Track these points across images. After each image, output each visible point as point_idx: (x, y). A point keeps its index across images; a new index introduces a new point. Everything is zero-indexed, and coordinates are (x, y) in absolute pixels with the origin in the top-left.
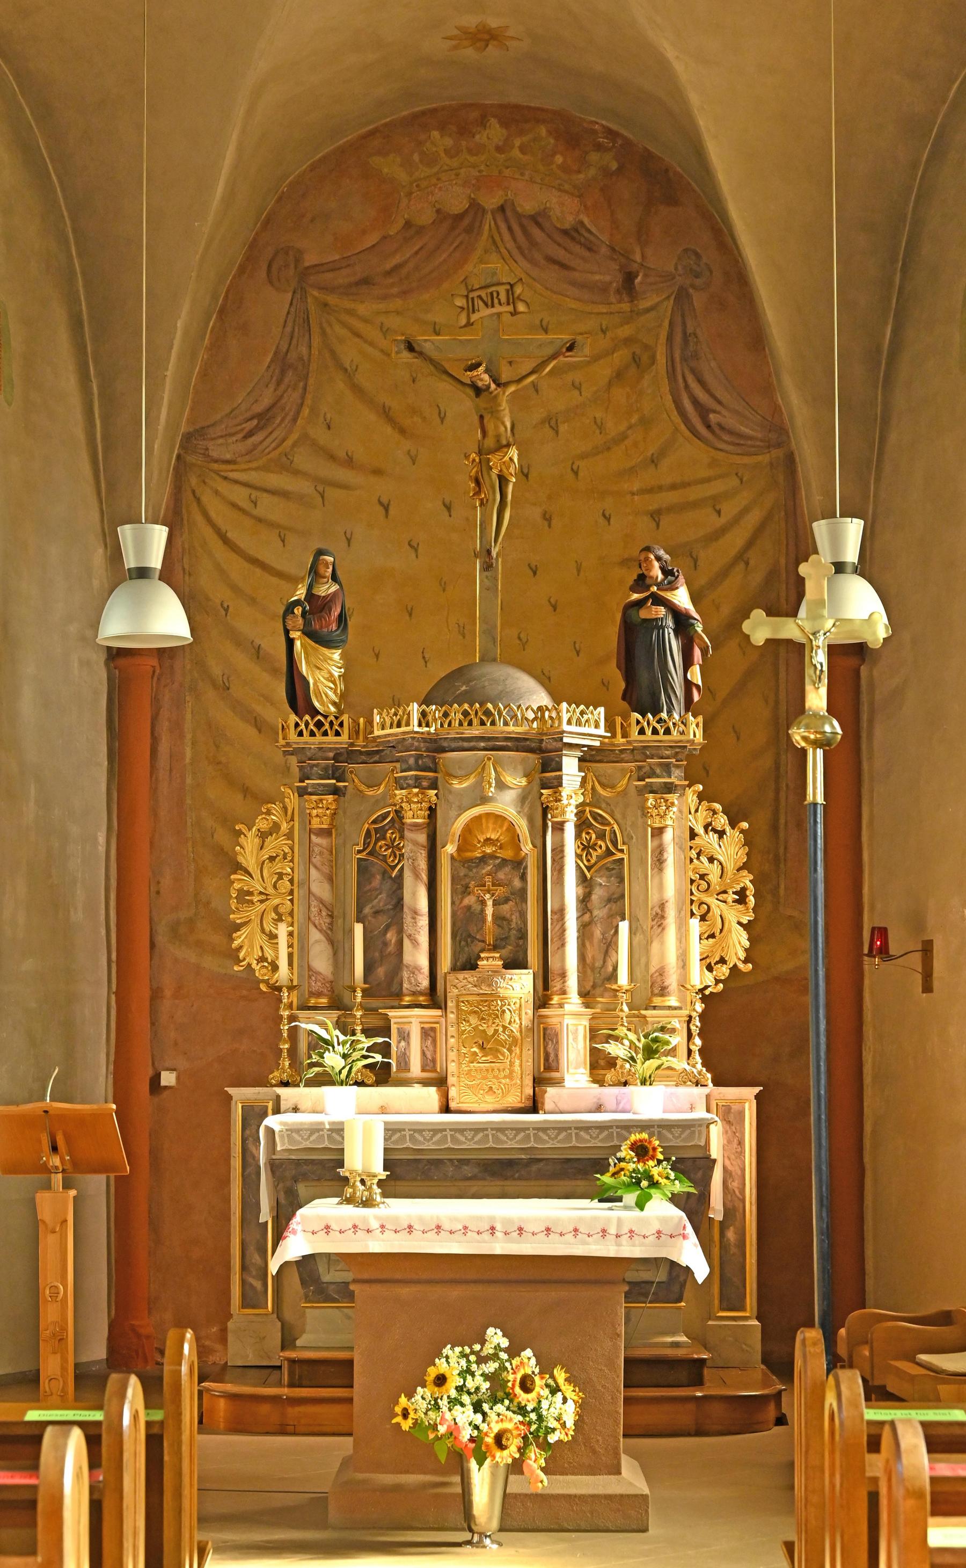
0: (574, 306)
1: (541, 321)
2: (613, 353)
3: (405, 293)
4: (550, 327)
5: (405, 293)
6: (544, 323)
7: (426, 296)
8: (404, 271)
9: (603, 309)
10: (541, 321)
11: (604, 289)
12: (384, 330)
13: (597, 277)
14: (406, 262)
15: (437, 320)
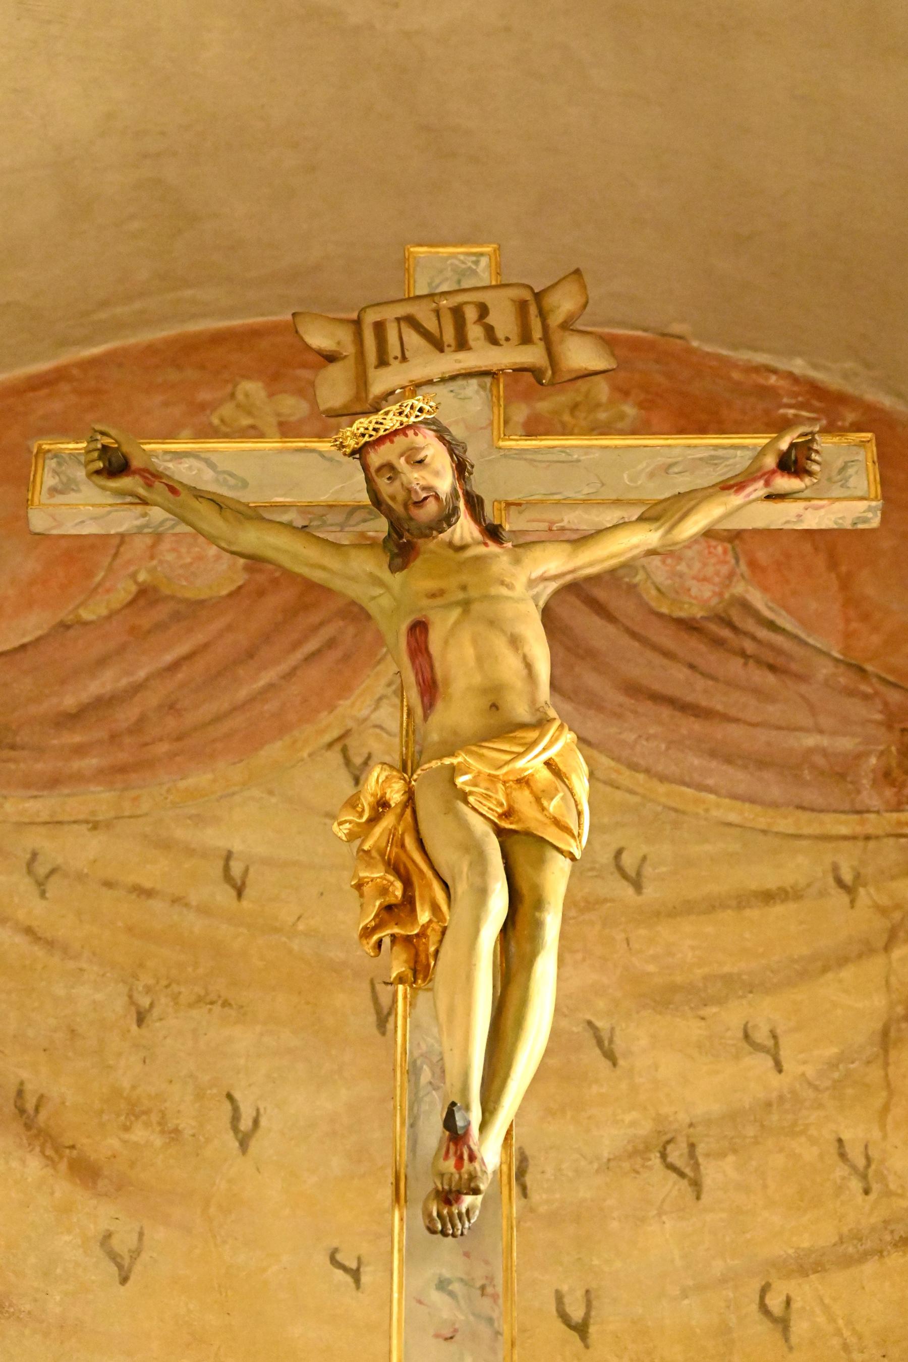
0: (733, 817)
1: (619, 853)
2: (887, 948)
3: (123, 769)
4: (648, 871)
5: (123, 769)
6: (628, 861)
7: (200, 779)
8: (126, 716)
9: (843, 825)
10: (619, 853)
11: (840, 772)
12: (41, 870)
13: (811, 741)
14: (137, 688)
15: (237, 846)
